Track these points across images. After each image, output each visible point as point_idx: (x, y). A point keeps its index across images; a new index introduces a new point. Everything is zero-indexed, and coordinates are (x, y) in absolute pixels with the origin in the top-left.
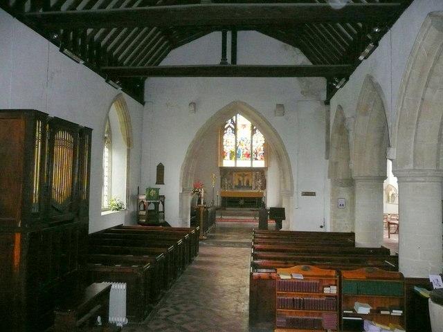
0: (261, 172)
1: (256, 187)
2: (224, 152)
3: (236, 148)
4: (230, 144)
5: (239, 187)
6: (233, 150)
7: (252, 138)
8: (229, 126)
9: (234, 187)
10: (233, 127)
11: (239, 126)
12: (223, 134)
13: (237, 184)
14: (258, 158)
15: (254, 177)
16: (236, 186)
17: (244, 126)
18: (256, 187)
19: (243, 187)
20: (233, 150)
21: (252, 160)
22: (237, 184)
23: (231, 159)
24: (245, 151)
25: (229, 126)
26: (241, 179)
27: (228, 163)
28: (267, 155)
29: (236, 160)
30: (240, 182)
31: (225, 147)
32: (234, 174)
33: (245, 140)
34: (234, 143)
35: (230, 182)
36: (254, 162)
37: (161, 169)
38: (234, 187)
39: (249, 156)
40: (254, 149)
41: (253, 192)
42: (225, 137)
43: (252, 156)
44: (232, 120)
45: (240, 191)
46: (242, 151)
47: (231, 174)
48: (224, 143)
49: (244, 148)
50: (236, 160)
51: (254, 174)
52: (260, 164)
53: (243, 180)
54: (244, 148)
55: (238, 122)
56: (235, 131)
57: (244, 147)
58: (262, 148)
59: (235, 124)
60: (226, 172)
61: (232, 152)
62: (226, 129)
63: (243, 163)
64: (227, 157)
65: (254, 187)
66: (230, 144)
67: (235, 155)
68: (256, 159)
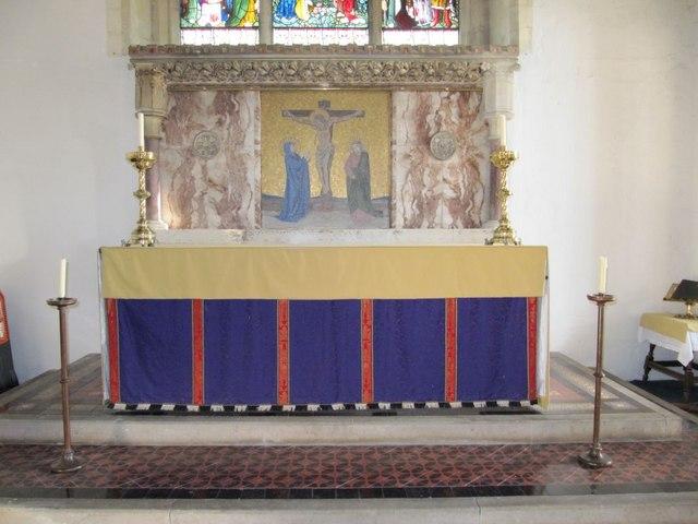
5: (292, 206)
9: (249, 210)
13: (278, 189)
14: (421, 13)
15: (404, 131)
16: (266, 202)
18: (425, 207)
21: (373, 28)
22: (278, 189)
30: (297, 169)
32: (250, 103)
35: (218, 166)
38: (249, 210)
45: (301, 236)
47: (226, 104)
51: (405, 102)
53: (326, 157)
65: (404, 208)
68: (405, 22)
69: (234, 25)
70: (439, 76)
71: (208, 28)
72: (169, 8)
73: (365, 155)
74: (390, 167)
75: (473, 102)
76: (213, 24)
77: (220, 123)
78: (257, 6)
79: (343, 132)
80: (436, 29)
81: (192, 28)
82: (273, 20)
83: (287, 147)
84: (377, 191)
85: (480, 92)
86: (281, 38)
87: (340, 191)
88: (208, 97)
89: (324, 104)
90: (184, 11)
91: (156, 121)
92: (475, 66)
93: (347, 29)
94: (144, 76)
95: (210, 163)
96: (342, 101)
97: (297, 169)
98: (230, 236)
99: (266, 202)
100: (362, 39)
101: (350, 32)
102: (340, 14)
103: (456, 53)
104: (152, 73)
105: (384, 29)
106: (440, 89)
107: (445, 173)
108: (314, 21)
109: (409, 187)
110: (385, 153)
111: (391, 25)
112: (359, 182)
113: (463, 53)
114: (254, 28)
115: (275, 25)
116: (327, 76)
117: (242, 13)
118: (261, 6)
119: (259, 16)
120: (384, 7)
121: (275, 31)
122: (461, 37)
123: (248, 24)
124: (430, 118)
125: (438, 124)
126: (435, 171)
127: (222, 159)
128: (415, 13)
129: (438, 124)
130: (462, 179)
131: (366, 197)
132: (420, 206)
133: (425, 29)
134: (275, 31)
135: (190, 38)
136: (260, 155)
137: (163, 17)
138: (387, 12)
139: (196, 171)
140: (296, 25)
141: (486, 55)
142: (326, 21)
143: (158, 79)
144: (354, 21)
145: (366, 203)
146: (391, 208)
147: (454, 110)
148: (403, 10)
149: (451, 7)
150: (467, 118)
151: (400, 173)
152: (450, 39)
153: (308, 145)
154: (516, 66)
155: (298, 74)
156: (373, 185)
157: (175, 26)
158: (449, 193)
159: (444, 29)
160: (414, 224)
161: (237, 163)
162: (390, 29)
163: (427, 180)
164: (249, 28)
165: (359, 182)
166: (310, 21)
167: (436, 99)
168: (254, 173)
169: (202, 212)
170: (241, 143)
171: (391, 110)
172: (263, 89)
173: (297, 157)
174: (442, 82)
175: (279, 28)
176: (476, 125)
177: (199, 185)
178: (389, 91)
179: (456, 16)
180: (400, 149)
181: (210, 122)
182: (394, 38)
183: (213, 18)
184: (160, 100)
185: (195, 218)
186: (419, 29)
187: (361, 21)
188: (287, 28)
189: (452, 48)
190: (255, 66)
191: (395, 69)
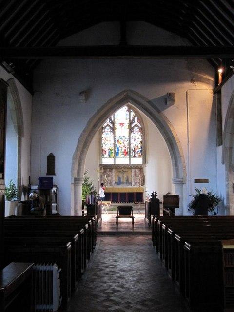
0: (140, 168)
1: (136, 183)
2: (103, 150)
4: (109, 143)
5: (119, 183)
6: (112, 147)
7: (129, 136)
8: (108, 125)
9: (113, 184)
10: (112, 126)
12: (101, 133)
13: (117, 181)
14: (137, 155)
15: (133, 174)
17: (122, 125)
18: (136, 183)
19: (123, 183)
21: (130, 157)
22: (117, 181)
23: (110, 156)
24: (124, 149)
25: (108, 125)
26: (121, 175)
27: (107, 161)
28: (144, 153)
29: (114, 158)
30: (119, 178)
32: (114, 170)
33: (124, 139)
34: (112, 142)
36: (132, 159)
37: (51, 159)
38: (113, 184)
39: (126, 153)
40: (132, 146)
41: (133, 187)
42: (104, 136)
43: (130, 154)
44: (110, 119)
45: (120, 186)
46: (120, 149)
47: (111, 171)
48: (103, 142)
49: (122, 146)
50: (114, 158)
52: (138, 161)
54: (122, 146)
56: (113, 129)
57: (123, 144)
58: (140, 146)
59: (113, 123)
60: (106, 168)
61: (110, 150)
63: (122, 160)
64: (107, 155)
65: (133, 184)
66: (109, 143)
67: (115, 153)
68: (134, 157)
79: (125, 174)
84: (130, 181)
87: (125, 181)
88: (108, 170)
90: (103, 155)
94: (101, 169)
97: (119, 178)
98: (111, 187)
112: (127, 180)
150: (141, 172)
153: (121, 175)
165: (127, 180)
167: (137, 170)
168: (114, 179)
178: (131, 169)
180: (132, 176)
184: (103, 171)
187: (128, 156)
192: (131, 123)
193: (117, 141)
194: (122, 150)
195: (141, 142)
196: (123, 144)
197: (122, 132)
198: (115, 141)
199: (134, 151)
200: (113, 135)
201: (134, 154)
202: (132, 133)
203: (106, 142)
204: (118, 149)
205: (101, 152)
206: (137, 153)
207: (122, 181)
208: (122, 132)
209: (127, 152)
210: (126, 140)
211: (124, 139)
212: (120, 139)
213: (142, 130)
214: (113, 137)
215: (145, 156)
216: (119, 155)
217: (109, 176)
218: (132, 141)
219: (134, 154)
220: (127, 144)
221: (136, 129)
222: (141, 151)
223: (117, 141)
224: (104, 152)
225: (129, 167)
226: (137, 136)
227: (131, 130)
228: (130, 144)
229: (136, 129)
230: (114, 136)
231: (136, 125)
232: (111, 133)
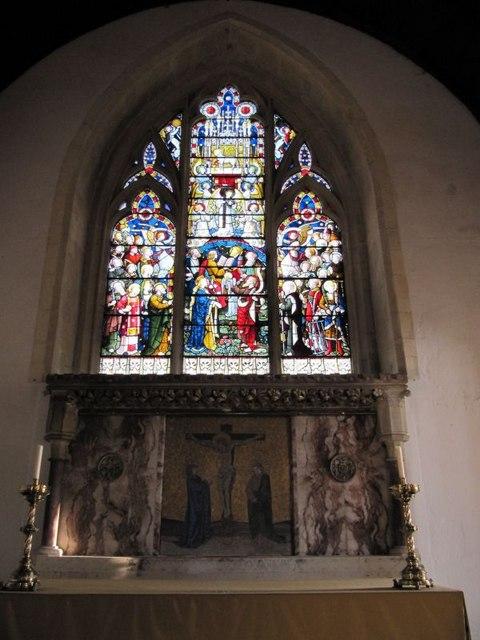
2: (109, 313)
3: (181, 286)
6: (163, 295)
7: (269, 236)
8: (147, 183)
9: (148, 535)
11: (202, 189)
13: (178, 514)
14: (317, 343)
15: (304, 453)
17: (227, 182)
18: (329, 532)
19: (227, 528)
20: (163, 295)
21: (275, 357)
24: (235, 305)
26: (210, 469)
29: (176, 356)
31: (118, 286)
32: (156, 428)
33: (235, 252)
34: (167, 263)
38: (148, 535)
39: (251, 330)
40: (287, 288)
44: (164, 149)
47: (133, 430)
49: (230, 293)
50: (176, 356)
51: (303, 426)
54: (230, 293)
55: (197, 166)
56: (177, 206)
58: (331, 287)
59: (180, 174)
61: (153, 317)
62: (131, 196)
65: (308, 533)
66: (147, 270)
67: (176, 322)
68: (302, 352)
69: (149, 354)
70: (333, 401)
71: (125, 356)
72: (91, 340)
73: (266, 478)
74: (292, 489)
75: (369, 426)
76: (130, 353)
77: (126, 446)
78: (170, 338)
80: (331, 357)
81: (111, 356)
82: (183, 350)
83: (189, 473)
84: (279, 515)
85: (375, 416)
86: (191, 367)
87: (243, 515)
88: (116, 421)
89: (227, 428)
90: (105, 341)
91: (63, 444)
92: (367, 392)
93: (249, 357)
95: (113, 485)
96: (243, 425)
97: (198, 491)
99: (167, 527)
100: (262, 368)
101: (252, 360)
102: (243, 345)
103: (349, 381)
104: (66, 400)
105: (284, 357)
106: (336, 413)
107: (347, 496)
108: (220, 350)
109: (311, 511)
110: (286, 476)
111: (290, 354)
112: (261, 504)
113: (355, 381)
114: (166, 357)
115: (186, 354)
116: (229, 402)
117: (157, 344)
118: (173, 338)
119: (172, 347)
120: (283, 338)
121: (186, 361)
122: (354, 364)
123: (161, 354)
124: (329, 440)
125: (337, 447)
126: (337, 494)
127: (124, 481)
128: (311, 344)
129: (337, 447)
130: (364, 501)
131: (268, 521)
132: (323, 531)
133: (320, 357)
134: (186, 361)
135: (109, 367)
136: (166, 479)
137: (85, 347)
138: (286, 342)
139: (98, 494)
140: (204, 354)
141: (377, 382)
142: (231, 351)
143: (70, 406)
144: (257, 351)
145: (270, 530)
146: (294, 533)
147: (351, 433)
148: (300, 341)
149: (342, 338)
151: (301, 496)
152: (342, 367)
154: (406, 393)
155: (201, 400)
156: (274, 508)
157: (95, 355)
158: (353, 517)
159: (338, 357)
160: (318, 551)
161: (140, 488)
162: (289, 357)
163: (329, 503)
164: (162, 357)
165: (261, 504)
166: (217, 351)
167: (333, 423)
168: (156, 496)
169: (99, 536)
170: (144, 466)
171: (291, 434)
172: (169, 415)
173: (198, 480)
174: (337, 407)
175: (189, 357)
176: (374, 446)
177: (100, 507)
178: (288, 416)
179: (348, 346)
180: (300, 471)
181: (115, 446)
182: (293, 367)
183: (131, 348)
184: (70, 425)
185: (91, 544)
186: (315, 357)
187: (262, 350)
188: (196, 357)
189: (345, 376)
190: (162, 393)
191: (293, 396)
192: (273, 176)
193: (194, 262)
194: (225, 309)
195: (339, 268)
196: (228, 280)
197: (226, 217)
198: (182, 262)
199: (297, 317)
200: (172, 233)
201: (302, 333)
202: (286, 222)
203: (132, 268)
204: (200, 308)
205: (97, 322)
206: (320, 330)
207: (216, 513)
208: (226, 217)
209: (259, 324)
210: (251, 257)
211: (235, 252)
212: (214, 254)
213: (345, 213)
214: (172, 239)
215: (375, 344)
216: (210, 342)
217: (115, 472)
218: (286, 266)
219: (302, 332)
220: (253, 280)
221: (308, 204)
222: (342, 319)
223: (194, 262)
224: (114, 323)
225: (271, 401)
226: (311, 257)
227: (277, 207)
228: (271, 279)
229: (308, 204)
230: (183, 237)
231: (306, 185)
232: (167, 222)
